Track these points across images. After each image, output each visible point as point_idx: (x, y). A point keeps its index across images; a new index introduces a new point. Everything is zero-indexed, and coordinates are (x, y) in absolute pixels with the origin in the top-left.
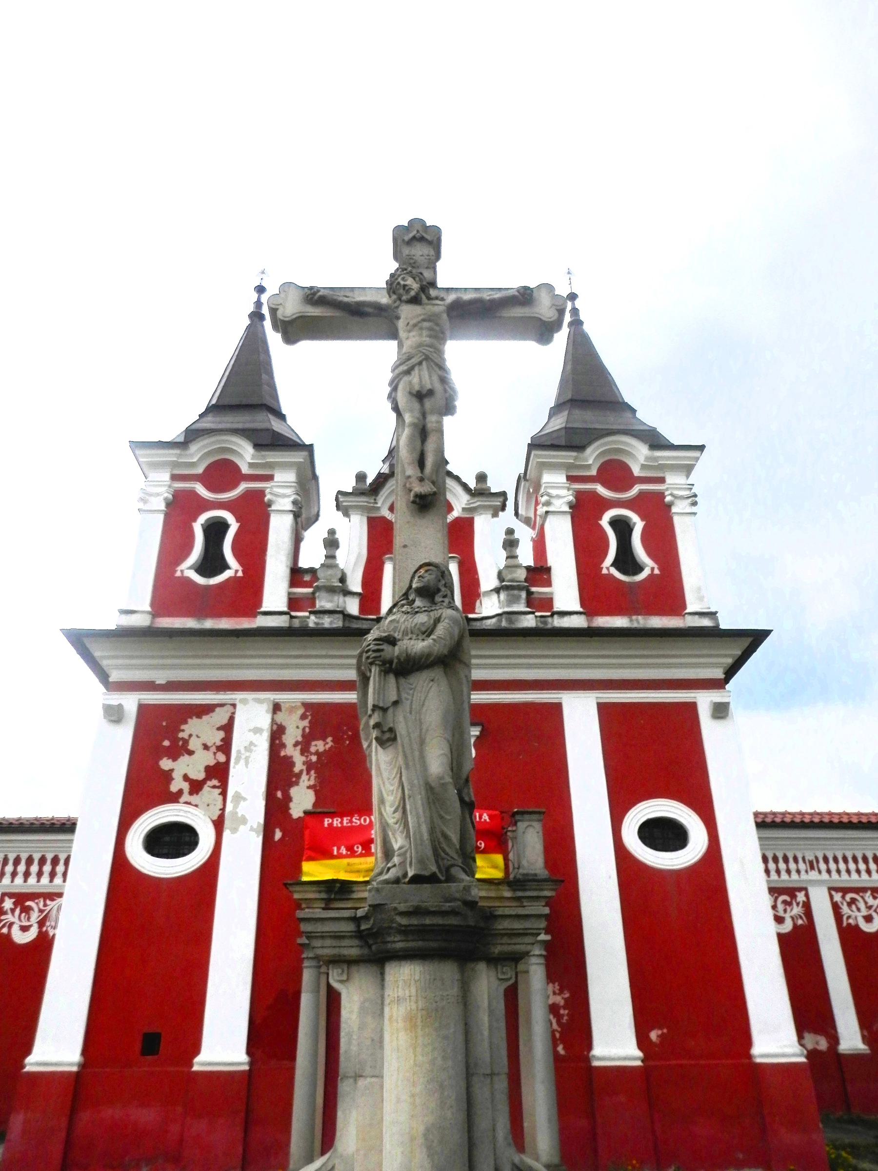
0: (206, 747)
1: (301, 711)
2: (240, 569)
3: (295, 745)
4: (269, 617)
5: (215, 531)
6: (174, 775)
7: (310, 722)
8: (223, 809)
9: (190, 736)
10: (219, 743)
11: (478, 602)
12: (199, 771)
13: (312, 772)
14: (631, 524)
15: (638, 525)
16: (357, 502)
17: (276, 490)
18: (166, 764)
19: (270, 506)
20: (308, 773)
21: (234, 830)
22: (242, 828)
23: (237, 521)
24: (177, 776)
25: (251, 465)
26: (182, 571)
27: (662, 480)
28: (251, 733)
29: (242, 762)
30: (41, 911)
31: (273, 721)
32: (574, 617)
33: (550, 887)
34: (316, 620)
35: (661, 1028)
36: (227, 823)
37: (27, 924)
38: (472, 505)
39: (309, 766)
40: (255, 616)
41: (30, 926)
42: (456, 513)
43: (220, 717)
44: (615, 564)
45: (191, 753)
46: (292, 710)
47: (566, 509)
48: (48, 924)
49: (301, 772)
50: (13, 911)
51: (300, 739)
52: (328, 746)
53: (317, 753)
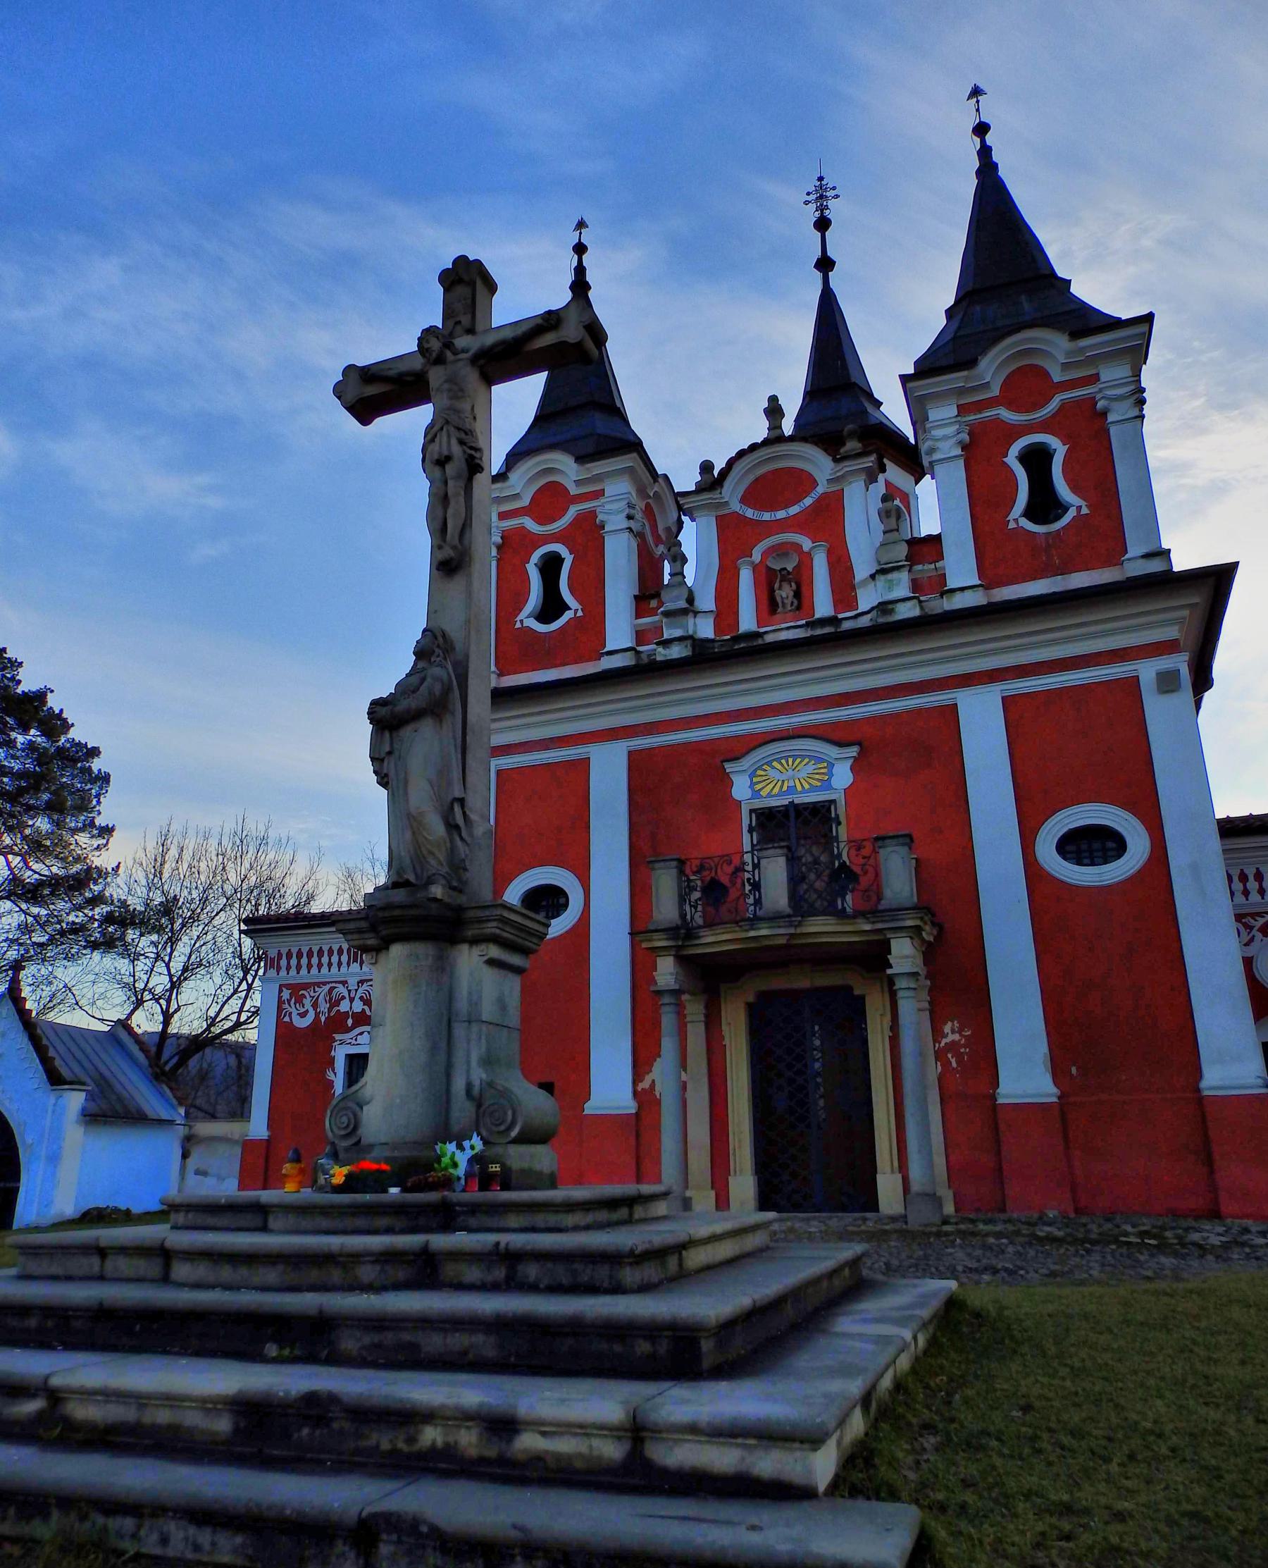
5: (551, 566)
14: (1052, 452)
15: (1060, 449)
17: (608, 507)
19: (603, 528)
25: (578, 483)
26: (522, 621)
27: (1095, 379)
32: (968, 593)
33: (915, 915)
38: (838, 474)
42: (820, 489)
44: (1029, 513)
47: (958, 451)
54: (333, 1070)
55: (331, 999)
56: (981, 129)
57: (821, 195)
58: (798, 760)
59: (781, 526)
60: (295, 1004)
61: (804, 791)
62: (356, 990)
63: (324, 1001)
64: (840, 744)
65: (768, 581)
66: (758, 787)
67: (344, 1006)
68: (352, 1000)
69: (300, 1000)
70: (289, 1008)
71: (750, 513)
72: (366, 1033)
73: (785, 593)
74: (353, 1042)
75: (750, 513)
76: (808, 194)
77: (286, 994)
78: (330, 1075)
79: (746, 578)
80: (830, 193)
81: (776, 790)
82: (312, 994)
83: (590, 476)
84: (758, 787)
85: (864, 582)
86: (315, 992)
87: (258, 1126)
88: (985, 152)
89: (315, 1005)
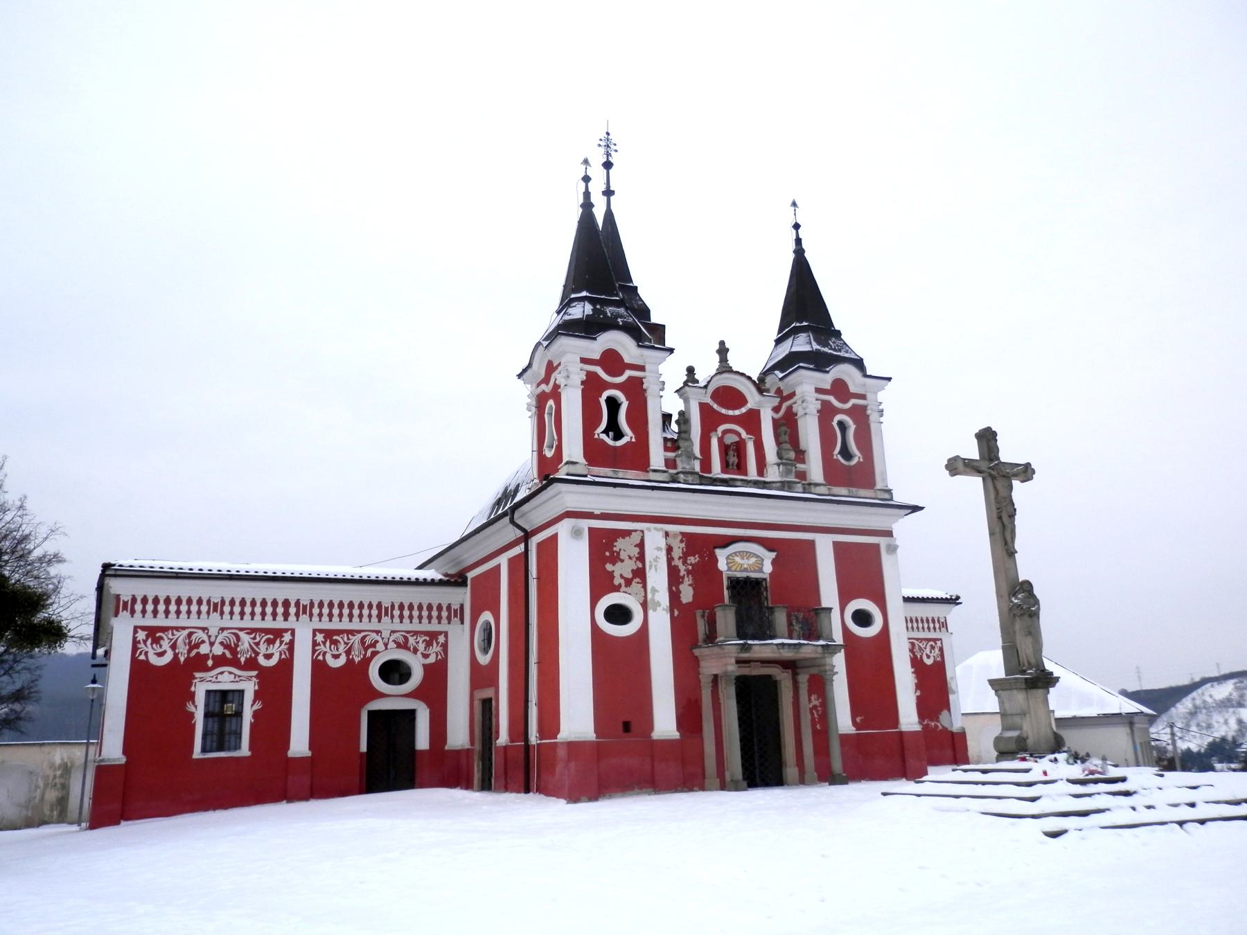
0: (630, 558)
1: (680, 537)
3: (680, 558)
4: (658, 474)
5: (613, 404)
6: (615, 574)
7: (685, 544)
8: (646, 596)
9: (620, 550)
10: (637, 555)
11: (765, 470)
12: (629, 573)
13: (690, 576)
14: (847, 426)
15: (852, 427)
18: (609, 567)
20: (688, 576)
21: (655, 610)
22: (658, 608)
23: (627, 400)
24: (617, 574)
27: (863, 397)
28: (656, 550)
29: (653, 568)
30: (345, 643)
31: (667, 544)
32: (822, 487)
34: (684, 478)
35: (861, 716)
36: (650, 605)
37: (338, 653)
39: (689, 572)
40: (648, 472)
41: (340, 654)
42: (750, 405)
43: (635, 538)
44: (840, 453)
45: (622, 561)
46: (675, 536)
48: (353, 653)
49: (684, 575)
50: (324, 643)
51: (681, 555)
52: (696, 561)
53: (691, 564)
54: (194, 703)
55: (190, 642)
56: (797, 226)
57: (608, 145)
58: (748, 554)
60: (152, 644)
61: (751, 572)
62: (216, 637)
63: (183, 646)
64: (771, 550)
65: (725, 449)
66: (730, 565)
67: (204, 649)
68: (212, 644)
69: (157, 641)
70: (145, 648)
71: (715, 406)
72: (226, 674)
73: (733, 459)
74: (214, 679)
75: (715, 406)
76: (601, 140)
77: (141, 635)
78: (191, 708)
79: (714, 443)
80: (612, 146)
81: (738, 569)
82: (170, 636)
84: (730, 565)
86: (173, 635)
87: (113, 748)
89: (174, 647)
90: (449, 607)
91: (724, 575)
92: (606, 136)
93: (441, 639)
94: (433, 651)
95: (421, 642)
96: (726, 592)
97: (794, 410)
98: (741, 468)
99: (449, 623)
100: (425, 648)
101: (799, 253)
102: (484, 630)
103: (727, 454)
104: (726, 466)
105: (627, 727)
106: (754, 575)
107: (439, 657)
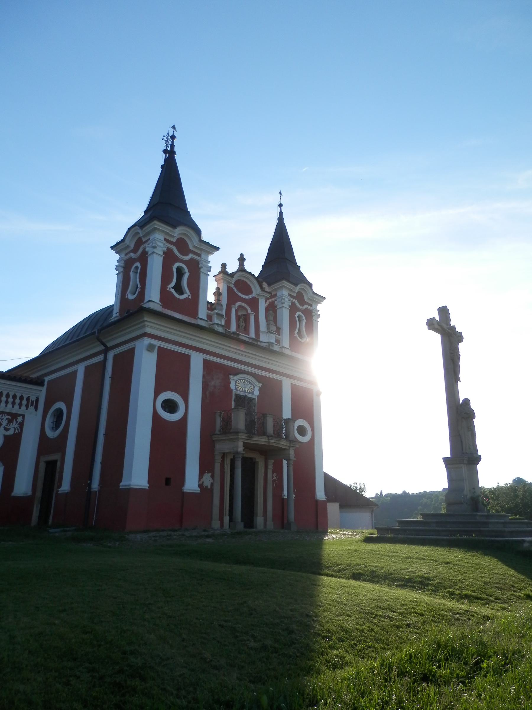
2: (190, 295)
16: (227, 278)
23: (189, 272)
25: (195, 247)
38: (260, 294)
40: (196, 319)
42: (254, 295)
56: (281, 205)
58: (247, 382)
59: (243, 300)
61: (249, 393)
64: (259, 382)
65: (238, 318)
66: (237, 387)
71: (236, 290)
73: (242, 324)
75: (236, 290)
76: (164, 136)
83: (199, 247)
84: (237, 387)
85: (263, 332)
88: (281, 213)
90: (28, 399)
91: (233, 392)
92: (167, 135)
93: (20, 419)
94: (13, 426)
95: (4, 419)
96: (233, 403)
97: (276, 303)
98: (246, 330)
99: (27, 409)
100: (7, 424)
101: (281, 219)
102: (54, 416)
103: (239, 320)
104: (238, 326)
105: (168, 481)
106: (249, 395)
107: (17, 431)
